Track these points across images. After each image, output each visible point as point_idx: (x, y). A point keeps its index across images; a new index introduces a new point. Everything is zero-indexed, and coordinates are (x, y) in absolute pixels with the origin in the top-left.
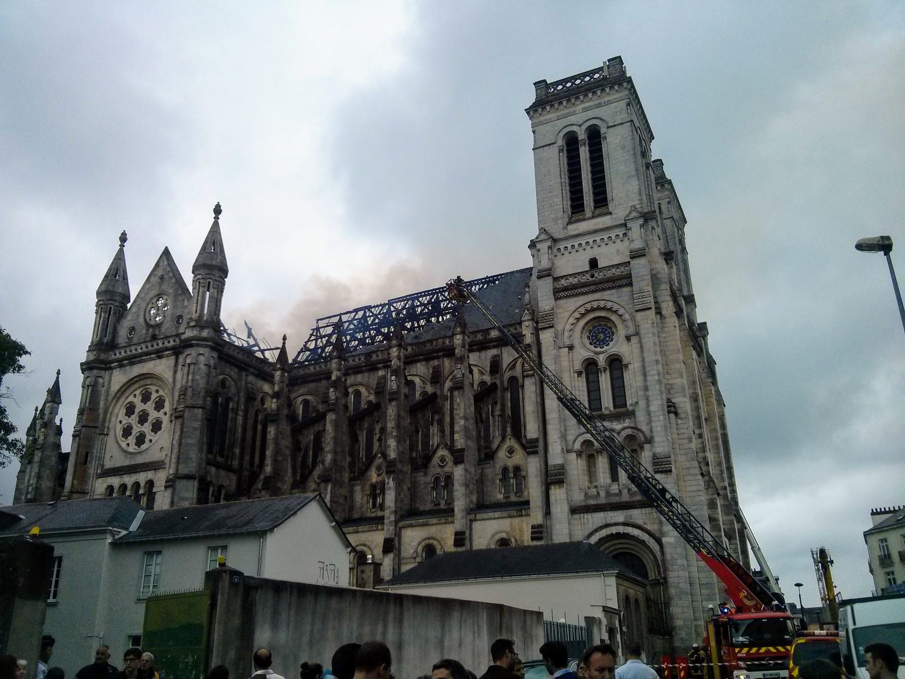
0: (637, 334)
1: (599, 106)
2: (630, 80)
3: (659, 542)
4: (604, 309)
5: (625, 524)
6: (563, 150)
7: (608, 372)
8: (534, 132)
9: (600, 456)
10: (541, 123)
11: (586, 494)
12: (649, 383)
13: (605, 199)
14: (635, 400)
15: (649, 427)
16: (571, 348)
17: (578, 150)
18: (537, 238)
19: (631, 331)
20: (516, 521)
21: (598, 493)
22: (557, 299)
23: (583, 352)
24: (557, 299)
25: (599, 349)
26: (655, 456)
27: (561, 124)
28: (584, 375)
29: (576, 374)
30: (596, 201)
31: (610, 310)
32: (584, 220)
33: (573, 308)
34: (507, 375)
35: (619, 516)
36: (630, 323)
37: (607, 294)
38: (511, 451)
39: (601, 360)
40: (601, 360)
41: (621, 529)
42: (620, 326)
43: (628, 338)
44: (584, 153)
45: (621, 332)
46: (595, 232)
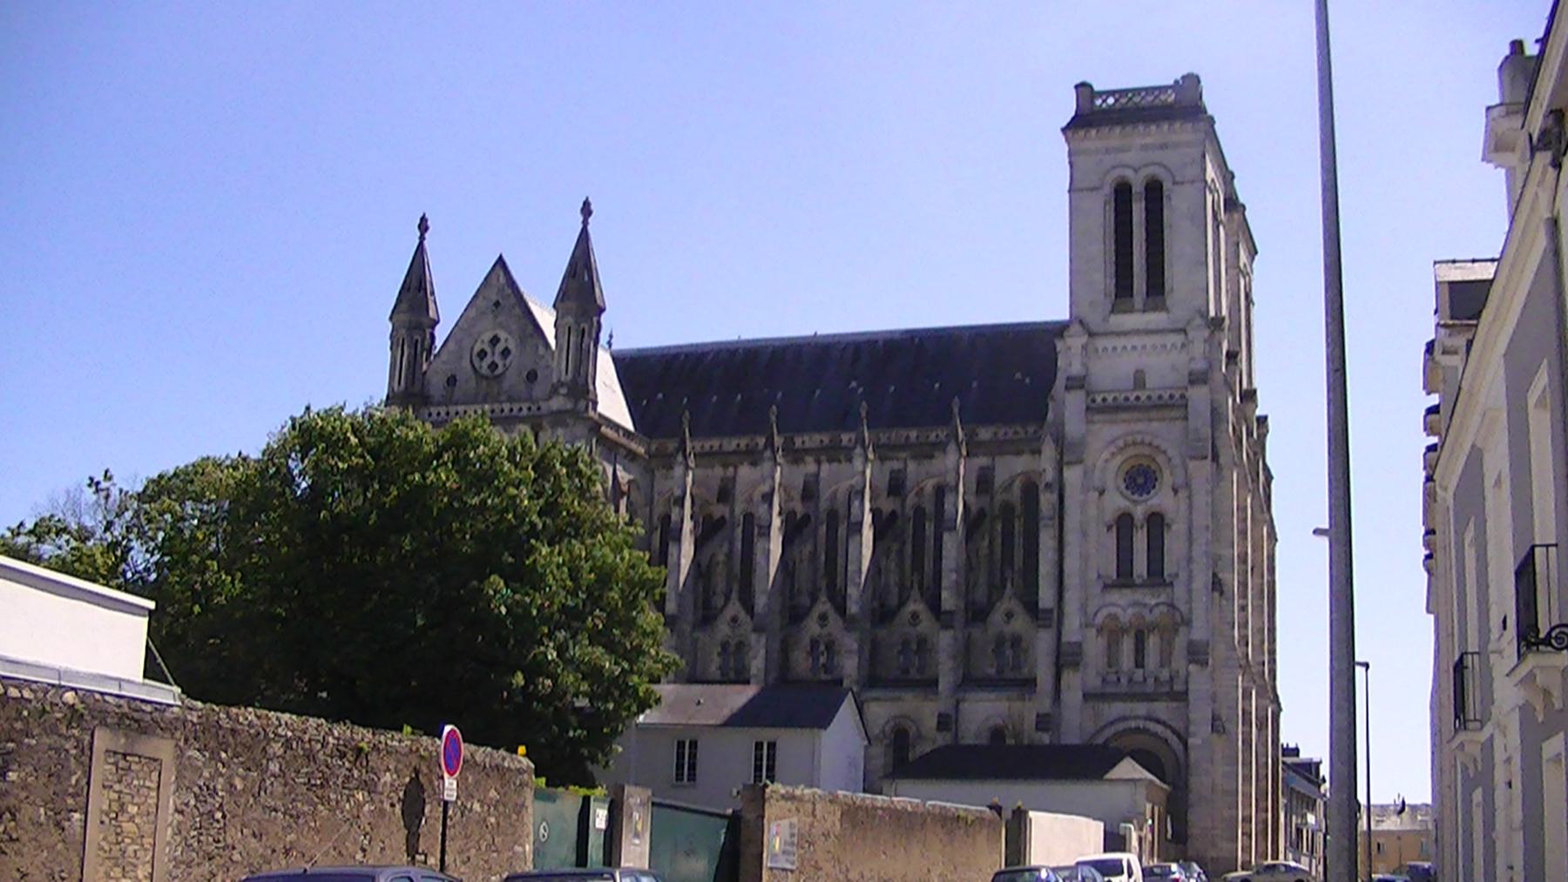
0: (1188, 485)
1: (1163, 146)
5: (1149, 718)
7: (1145, 529)
9: (1125, 636)
11: (1104, 680)
12: (1194, 554)
14: (1174, 570)
15: (1188, 606)
20: (1019, 704)
21: (1119, 679)
22: (1089, 422)
23: (1117, 501)
24: (1089, 422)
25: (1136, 497)
27: (1109, 160)
28: (1114, 529)
34: (999, 498)
35: (1141, 708)
36: (1180, 472)
38: (1009, 615)
39: (1139, 512)
40: (1139, 512)
41: (1141, 724)
42: (1166, 474)
45: (1167, 479)
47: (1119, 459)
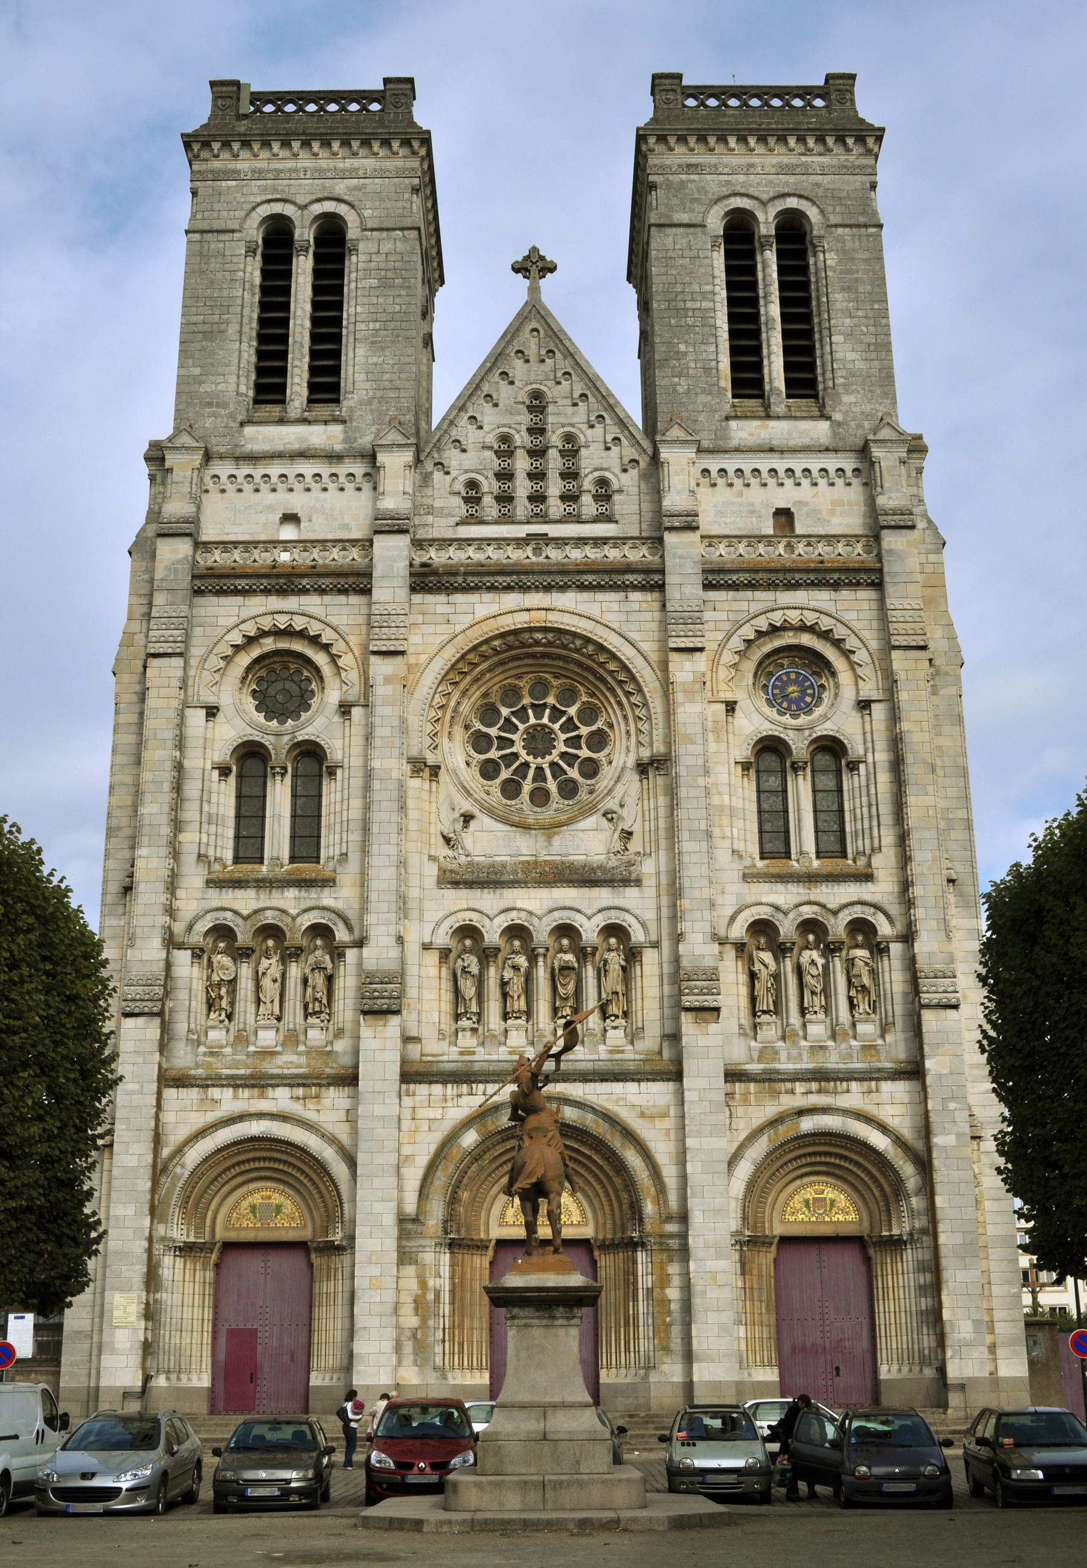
2: (426, 139)
3: (352, 1162)
4: (302, 634)
6: (254, 252)
7: (288, 778)
8: (194, 193)
10: (219, 176)
13: (335, 388)
16: (212, 712)
17: (289, 260)
18: (170, 439)
19: (354, 693)
26: (368, 979)
27: (256, 190)
28: (232, 779)
29: (216, 773)
30: (312, 387)
31: (315, 641)
32: (282, 421)
33: (234, 620)
37: (312, 603)
43: (345, 709)
44: (303, 268)
45: (333, 695)
46: (303, 455)
47: (244, 660)
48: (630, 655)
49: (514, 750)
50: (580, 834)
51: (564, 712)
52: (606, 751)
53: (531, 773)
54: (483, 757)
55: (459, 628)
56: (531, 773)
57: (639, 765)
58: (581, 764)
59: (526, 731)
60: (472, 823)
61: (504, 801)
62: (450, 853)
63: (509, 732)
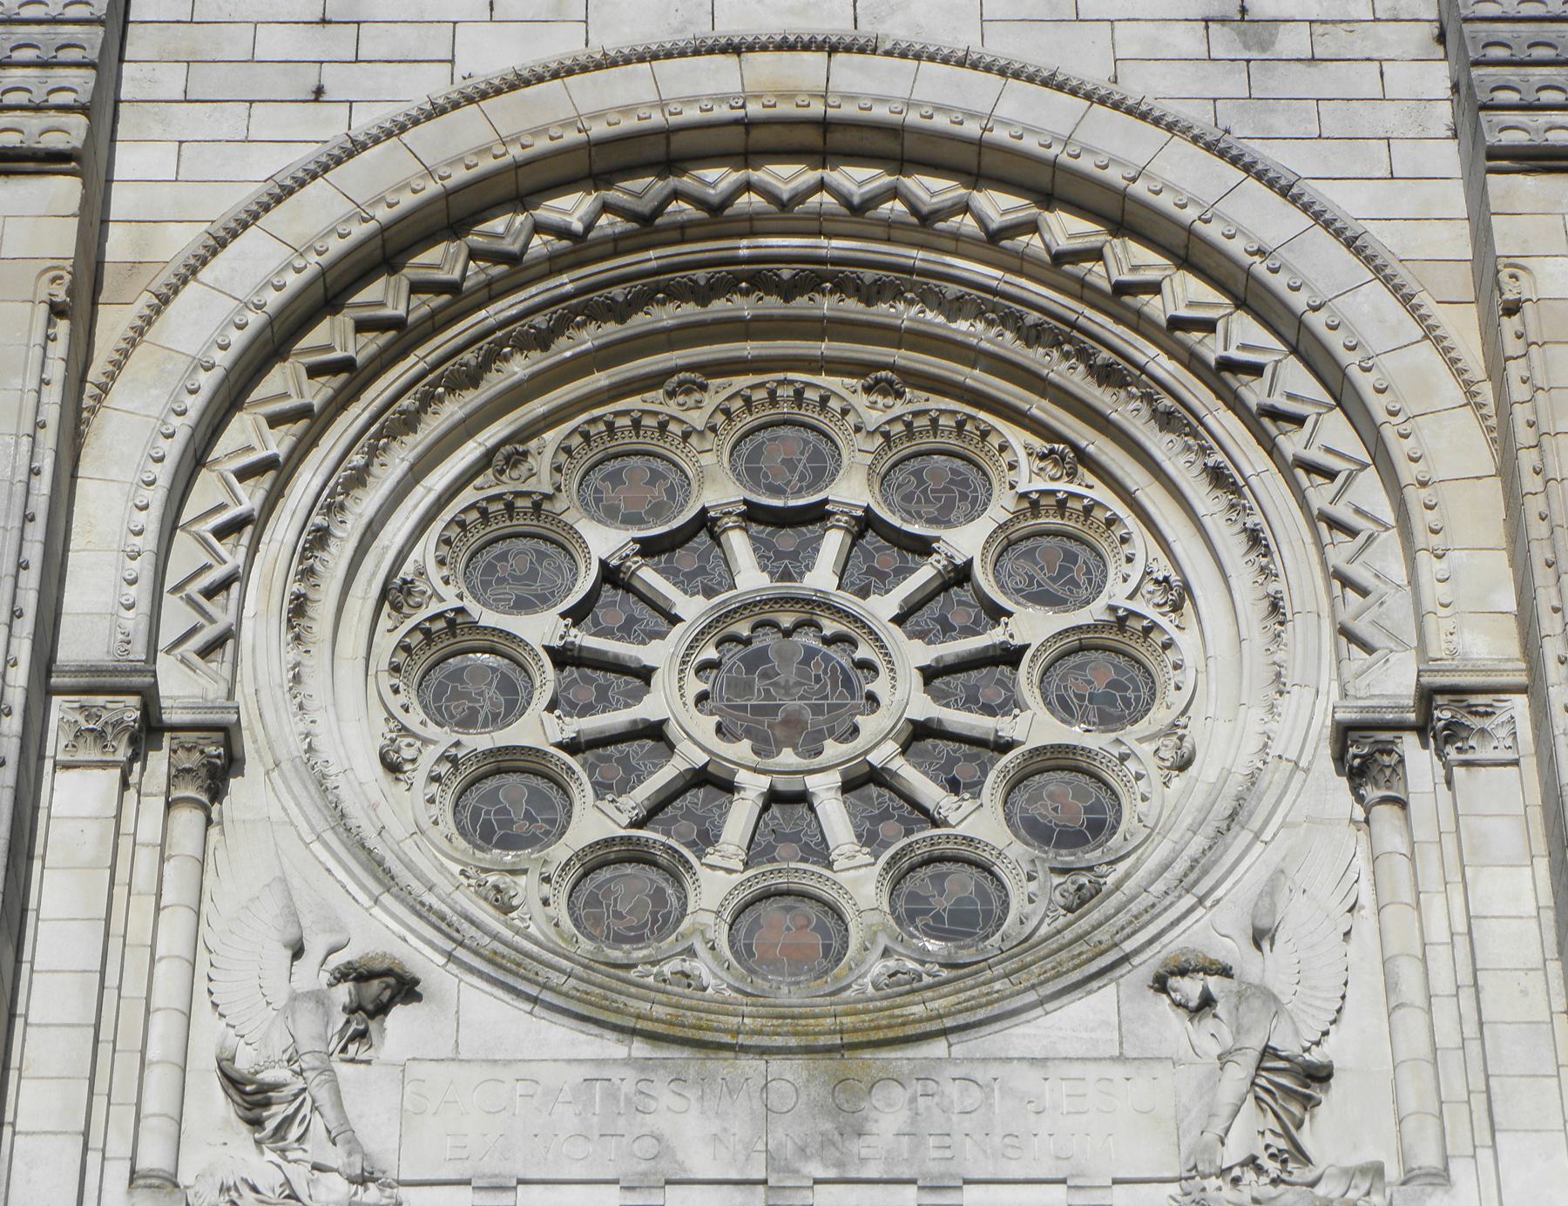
48: (1271, 237)
49: (650, 708)
50: (1026, 1079)
51: (923, 547)
52: (1159, 716)
53: (740, 818)
54: (481, 741)
55: (366, 120)
56: (740, 818)
57: (1345, 733)
58: (1015, 783)
59: (717, 627)
60: (399, 1015)
61: (586, 945)
62: (262, 1167)
63: (627, 631)
